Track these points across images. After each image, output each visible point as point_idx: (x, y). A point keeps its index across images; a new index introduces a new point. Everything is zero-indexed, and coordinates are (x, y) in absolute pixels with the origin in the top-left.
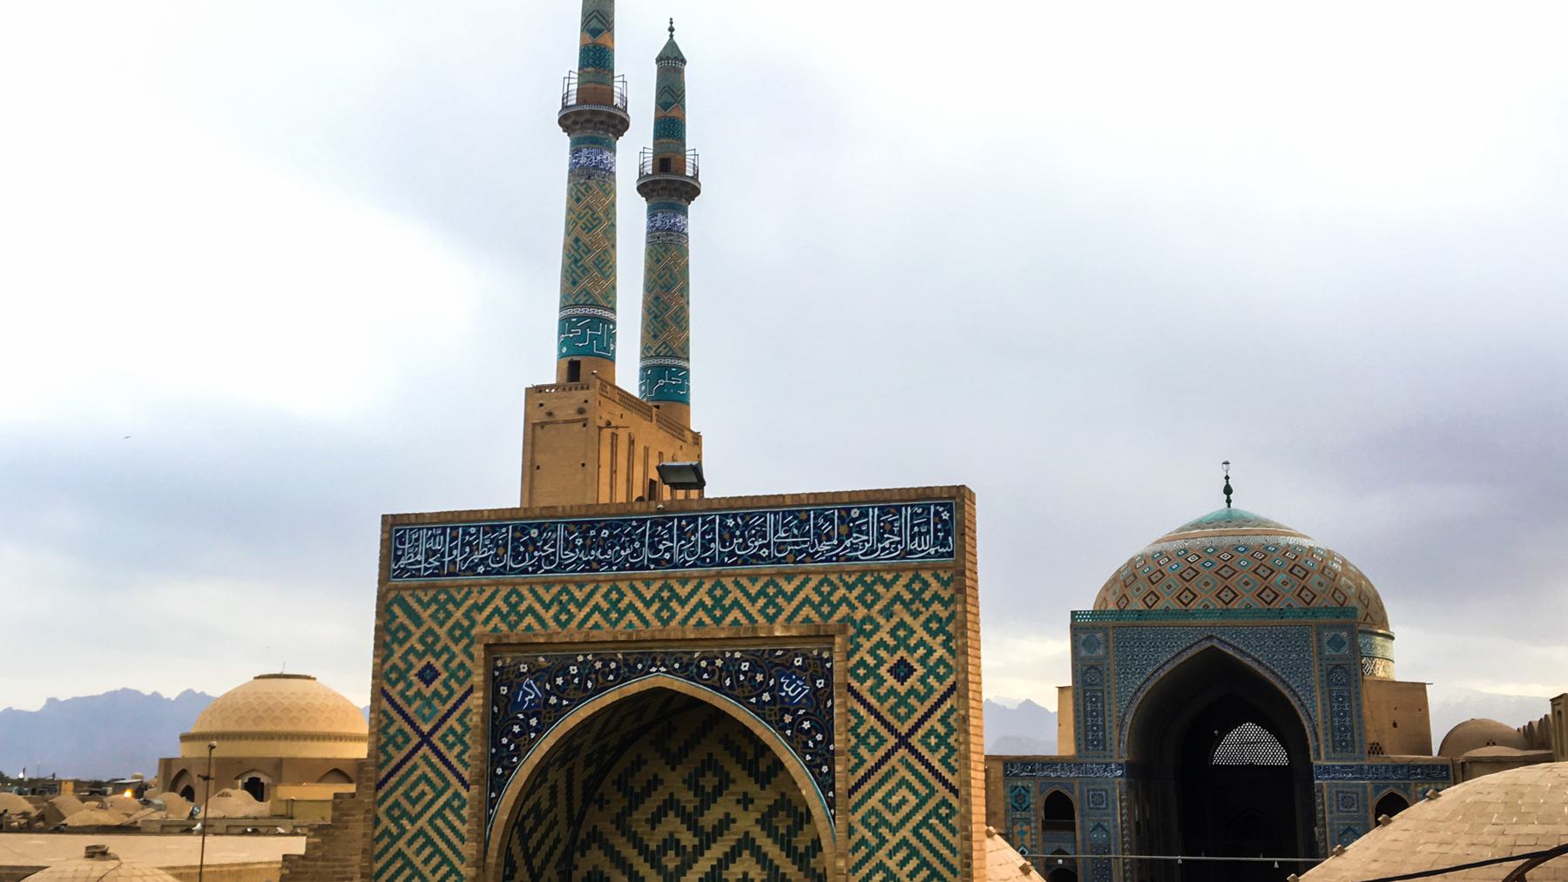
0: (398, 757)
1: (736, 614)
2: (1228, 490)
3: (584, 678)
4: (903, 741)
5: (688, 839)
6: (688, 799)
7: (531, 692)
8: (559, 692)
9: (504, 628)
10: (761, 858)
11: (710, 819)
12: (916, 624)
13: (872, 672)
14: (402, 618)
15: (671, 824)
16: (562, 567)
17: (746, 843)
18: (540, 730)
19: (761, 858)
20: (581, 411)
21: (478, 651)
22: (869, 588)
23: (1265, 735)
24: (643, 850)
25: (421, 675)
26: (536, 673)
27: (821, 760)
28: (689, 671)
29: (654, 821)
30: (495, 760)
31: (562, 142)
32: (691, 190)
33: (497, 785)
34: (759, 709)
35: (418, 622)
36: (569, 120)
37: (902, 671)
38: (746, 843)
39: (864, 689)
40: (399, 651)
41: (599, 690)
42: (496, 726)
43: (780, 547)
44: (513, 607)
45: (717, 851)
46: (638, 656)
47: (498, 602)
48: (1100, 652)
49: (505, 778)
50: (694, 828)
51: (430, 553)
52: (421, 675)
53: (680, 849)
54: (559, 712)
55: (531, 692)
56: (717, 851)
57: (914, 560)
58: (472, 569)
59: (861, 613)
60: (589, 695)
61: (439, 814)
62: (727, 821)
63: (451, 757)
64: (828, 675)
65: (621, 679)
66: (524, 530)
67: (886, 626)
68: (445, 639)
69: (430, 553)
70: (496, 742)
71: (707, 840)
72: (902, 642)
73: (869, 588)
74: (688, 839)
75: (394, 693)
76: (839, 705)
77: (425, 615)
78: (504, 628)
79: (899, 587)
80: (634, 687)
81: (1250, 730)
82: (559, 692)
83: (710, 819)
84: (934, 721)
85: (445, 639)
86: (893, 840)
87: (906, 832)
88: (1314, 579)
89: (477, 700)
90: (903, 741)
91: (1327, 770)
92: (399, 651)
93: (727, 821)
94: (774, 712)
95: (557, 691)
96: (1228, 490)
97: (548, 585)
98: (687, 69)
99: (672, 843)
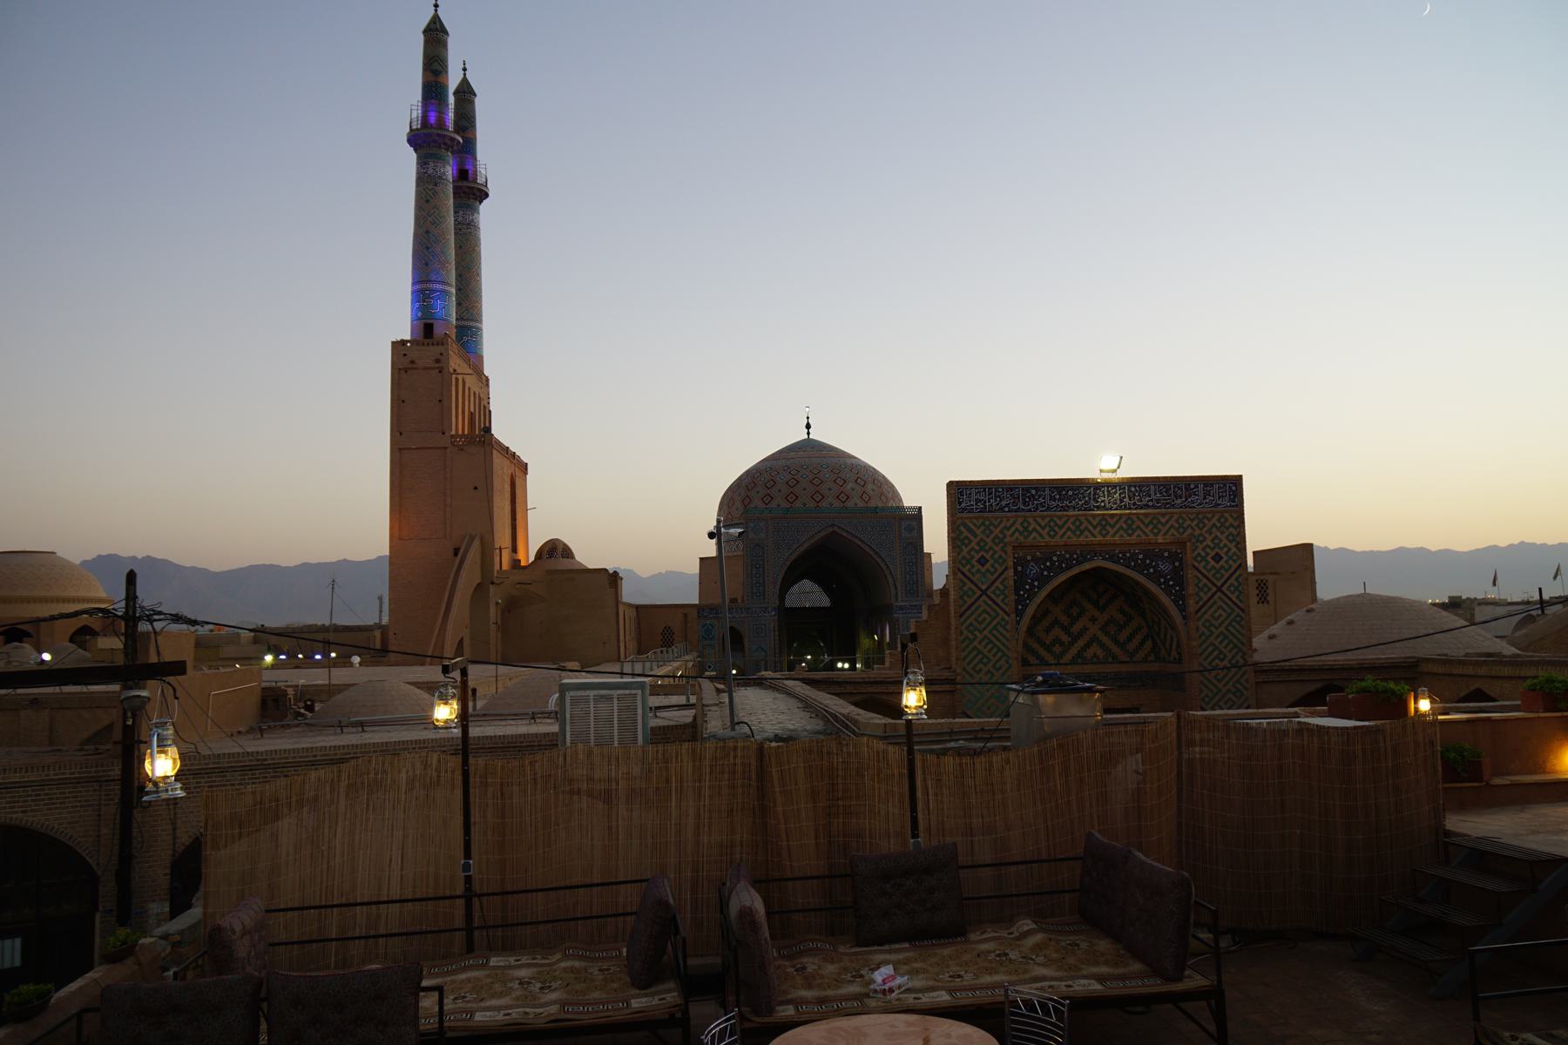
0: (970, 601)
1: (1138, 532)
2: (808, 426)
3: (1061, 563)
4: (1219, 589)
5: (1065, 639)
6: (1064, 619)
7: (1034, 569)
8: (1049, 569)
9: (1021, 538)
10: (1102, 646)
11: (1075, 629)
12: (1222, 537)
13: (1204, 559)
14: (966, 533)
15: (1057, 631)
16: (1049, 509)
17: (1095, 639)
18: (1039, 588)
19: (1102, 646)
20: (438, 361)
21: (1009, 549)
22: (1201, 521)
23: (816, 587)
24: (1042, 644)
25: (979, 561)
26: (1035, 559)
27: (1180, 599)
28: (1113, 558)
29: (1048, 630)
30: (1017, 602)
31: (410, 157)
32: (483, 195)
33: (1020, 614)
34: (1148, 576)
35: (975, 535)
36: (415, 139)
37: (1217, 558)
38: (1095, 639)
39: (1201, 566)
40: (965, 550)
41: (1068, 568)
42: (1018, 587)
43: (1158, 501)
44: (1025, 529)
45: (1080, 643)
46: (1089, 551)
47: (1017, 525)
48: (762, 535)
49: (1024, 610)
50: (1068, 633)
51: (977, 501)
52: (979, 561)
53: (1062, 644)
54: (1049, 579)
55: (1034, 569)
56: (1080, 643)
57: (1220, 508)
58: (1002, 509)
59: (1197, 532)
60: (1063, 571)
61: (995, 628)
62: (1085, 629)
63: (998, 601)
64: (1181, 560)
65: (1079, 563)
66: (1028, 490)
67: (1209, 538)
68: (990, 544)
69: (977, 501)
70: (1017, 593)
71: (1075, 639)
72: (1217, 545)
73: (1201, 521)
74: (1065, 639)
75: (965, 570)
76: (1190, 574)
77: (978, 532)
78: (1021, 538)
79: (1214, 520)
80: (1087, 566)
81: (807, 584)
82: (1049, 569)
83: (1075, 629)
84: (1232, 580)
85: (990, 544)
86: (1217, 632)
87: (1222, 629)
88: (870, 487)
89: (1011, 572)
90: (1219, 589)
91: (901, 608)
92: (965, 550)
93: (1085, 629)
94: (1156, 577)
95: (1047, 568)
96: (808, 426)
97: (1043, 518)
98: (477, 101)
99: (1057, 641)
